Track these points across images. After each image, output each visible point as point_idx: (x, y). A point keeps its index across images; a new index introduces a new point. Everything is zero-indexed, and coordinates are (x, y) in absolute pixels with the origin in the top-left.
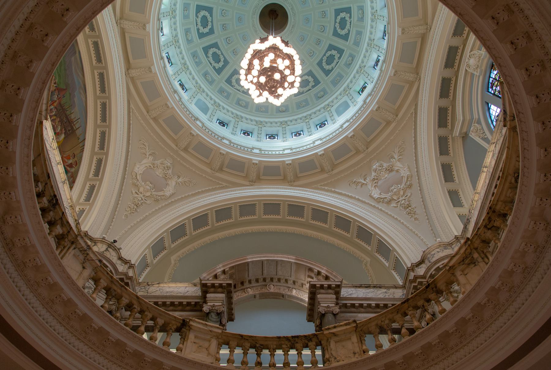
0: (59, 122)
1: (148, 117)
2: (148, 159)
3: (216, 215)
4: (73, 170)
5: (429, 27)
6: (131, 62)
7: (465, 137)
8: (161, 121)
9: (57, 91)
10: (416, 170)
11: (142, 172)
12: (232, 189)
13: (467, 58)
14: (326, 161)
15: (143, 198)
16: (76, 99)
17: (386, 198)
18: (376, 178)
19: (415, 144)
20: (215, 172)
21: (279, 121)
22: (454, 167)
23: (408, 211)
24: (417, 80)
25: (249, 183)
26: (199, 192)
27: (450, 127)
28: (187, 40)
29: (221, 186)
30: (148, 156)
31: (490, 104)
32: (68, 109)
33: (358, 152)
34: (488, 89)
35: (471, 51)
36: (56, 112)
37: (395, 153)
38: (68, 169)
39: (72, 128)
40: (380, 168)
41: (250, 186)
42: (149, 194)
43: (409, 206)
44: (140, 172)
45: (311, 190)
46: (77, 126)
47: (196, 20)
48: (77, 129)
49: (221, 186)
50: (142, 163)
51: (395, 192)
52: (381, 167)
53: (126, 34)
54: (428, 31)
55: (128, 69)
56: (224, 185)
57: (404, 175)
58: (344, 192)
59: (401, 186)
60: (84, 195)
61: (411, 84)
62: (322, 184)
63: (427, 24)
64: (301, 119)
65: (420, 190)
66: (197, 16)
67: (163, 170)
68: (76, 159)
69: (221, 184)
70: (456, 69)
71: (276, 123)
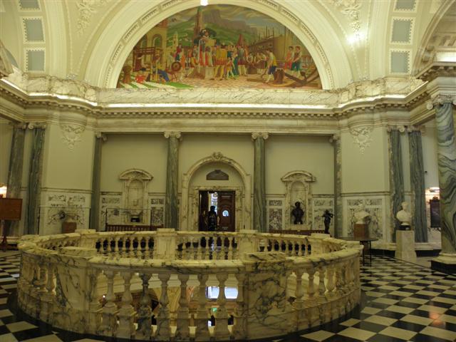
16: (252, 25)
38: (298, 59)
39: (270, 40)
68: (294, 47)
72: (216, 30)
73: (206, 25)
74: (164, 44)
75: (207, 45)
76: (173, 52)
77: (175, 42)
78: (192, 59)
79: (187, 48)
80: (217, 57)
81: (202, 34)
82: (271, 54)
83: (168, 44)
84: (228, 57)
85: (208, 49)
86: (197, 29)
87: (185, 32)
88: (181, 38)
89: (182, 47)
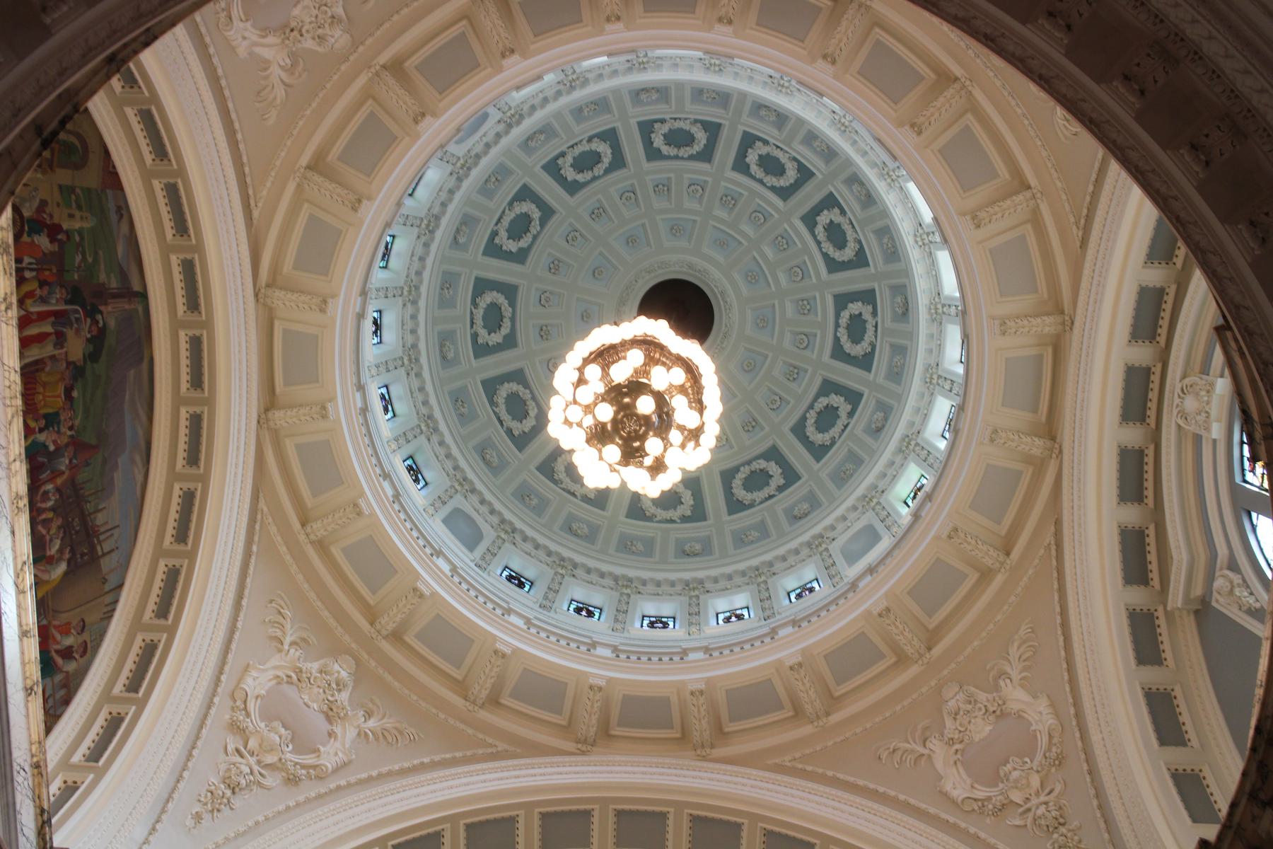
0: (59, 528)
1: (302, 537)
2: (287, 654)
3: (468, 838)
4: (71, 667)
5: (1067, 318)
6: (278, 390)
7: (1203, 611)
8: (336, 551)
9: (71, 449)
10: (1072, 711)
11: (263, 692)
12: (522, 761)
13: (1176, 395)
14: (808, 685)
15: (256, 768)
16: (118, 477)
17: (989, 799)
18: (956, 737)
19: (1063, 634)
20: (476, 708)
21: (680, 580)
22: (1180, 701)
23: (1057, 841)
24: (1054, 456)
25: (574, 745)
26: (422, 764)
27: (1156, 582)
28: (444, 358)
29: (490, 750)
30: (286, 647)
31: (1254, 515)
32: (90, 499)
33: (902, 660)
34: (1244, 475)
35: (1184, 377)
36: (56, 501)
37: (1010, 663)
38: (59, 660)
39: (92, 548)
40: (969, 707)
41: (578, 754)
42: (275, 759)
43: (1060, 824)
44: (257, 691)
45: (761, 773)
46: (107, 547)
47: (472, 313)
48: (104, 555)
49: (490, 750)
50: (268, 665)
51: (1016, 781)
52: (970, 703)
53: (277, 323)
54: (1067, 328)
55: (267, 410)
56: (499, 749)
57: (1041, 727)
58: (861, 782)
59: (1032, 761)
60: (88, 742)
61: (1039, 466)
62: (798, 755)
63: (1062, 312)
64: (743, 574)
65: (1090, 773)
66: (474, 304)
67: (324, 692)
69: (491, 745)
70: (1153, 425)
71: (673, 584)
72: (104, 358)
73: (112, 323)
74: (63, 176)
75: (70, 333)
76: (48, 210)
77: (71, 216)
78: (35, 285)
79: (58, 259)
80: (43, 377)
81: (92, 312)
82: (63, 567)
83: (66, 191)
84: (46, 416)
85: (60, 339)
86: (102, 294)
87: (96, 253)
88: (82, 238)
89: (61, 242)
